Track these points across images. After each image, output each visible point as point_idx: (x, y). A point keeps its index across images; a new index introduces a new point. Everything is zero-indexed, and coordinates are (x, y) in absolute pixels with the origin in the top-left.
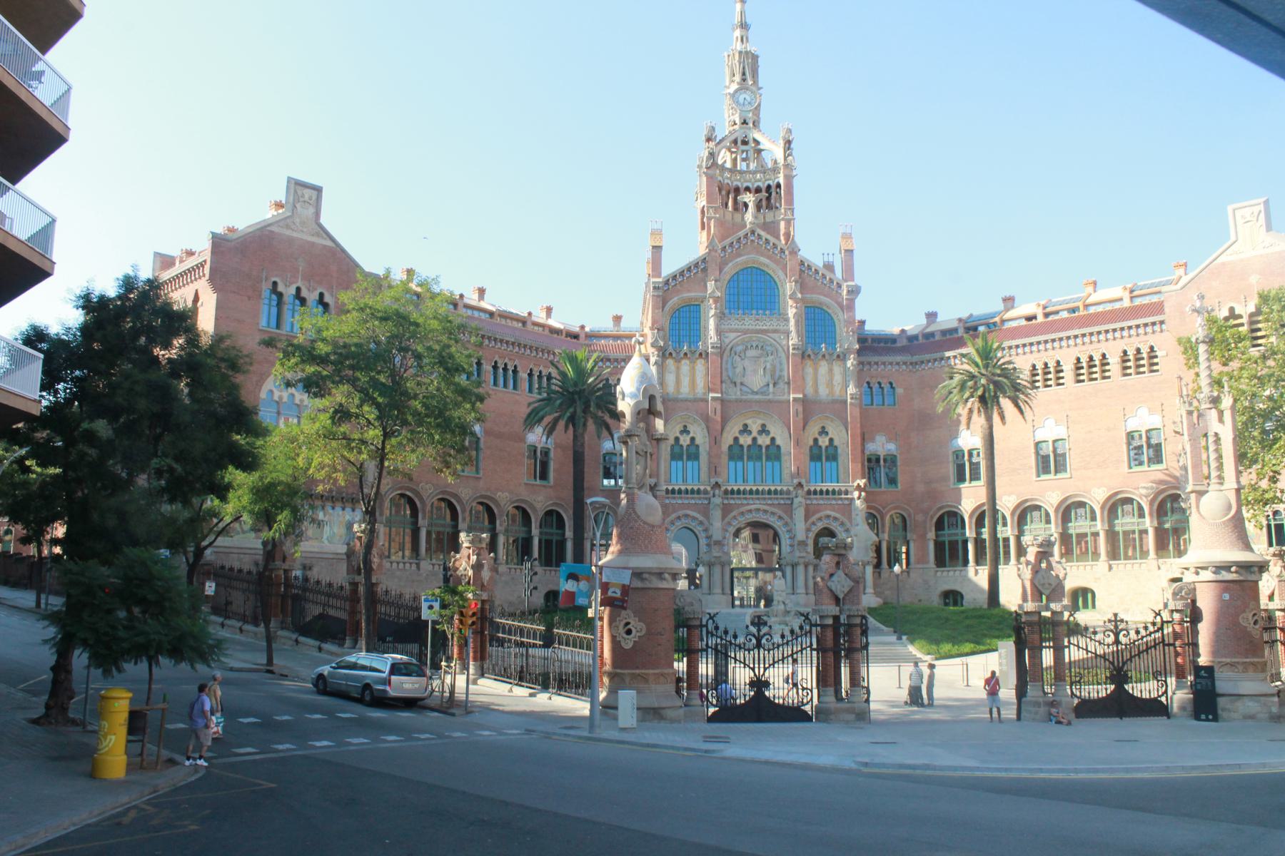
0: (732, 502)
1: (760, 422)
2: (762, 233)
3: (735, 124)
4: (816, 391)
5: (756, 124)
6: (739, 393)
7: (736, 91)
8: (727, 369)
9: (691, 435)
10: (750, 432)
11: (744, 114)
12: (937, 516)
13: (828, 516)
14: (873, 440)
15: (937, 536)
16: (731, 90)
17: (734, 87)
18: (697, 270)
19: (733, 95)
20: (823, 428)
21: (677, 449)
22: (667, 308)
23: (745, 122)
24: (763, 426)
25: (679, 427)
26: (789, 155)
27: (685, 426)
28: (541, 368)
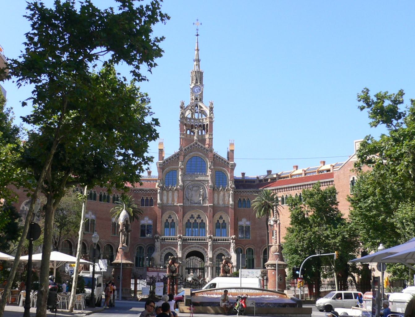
0: (186, 243)
1: (197, 214)
2: (200, 144)
3: (193, 100)
4: (218, 203)
5: (201, 100)
6: (190, 203)
7: (193, 87)
8: (186, 195)
9: (172, 219)
10: (194, 218)
11: (196, 96)
12: (264, 249)
13: (221, 249)
14: (241, 220)
15: (264, 257)
16: (192, 87)
17: (193, 85)
18: (175, 158)
19: (192, 89)
20: (221, 216)
21: (167, 224)
22: (164, 172)
23: (197, 99)
24: (199, 215)
25: (168, 216)
26: (211, 113)
27: (170, 216)
28: (118, 194)
